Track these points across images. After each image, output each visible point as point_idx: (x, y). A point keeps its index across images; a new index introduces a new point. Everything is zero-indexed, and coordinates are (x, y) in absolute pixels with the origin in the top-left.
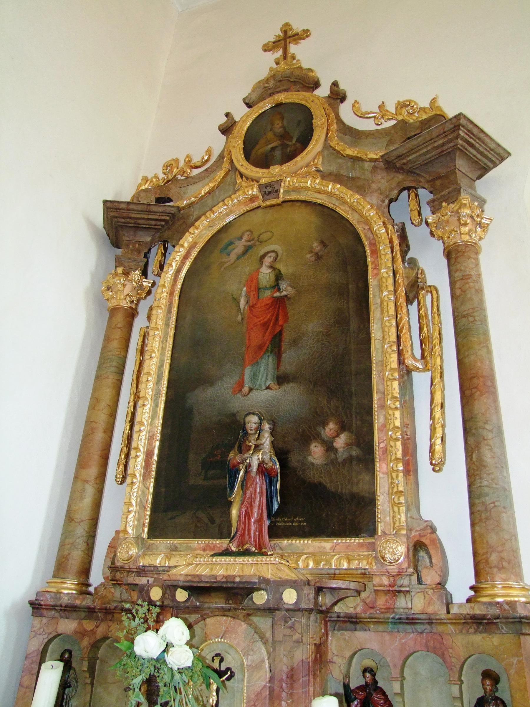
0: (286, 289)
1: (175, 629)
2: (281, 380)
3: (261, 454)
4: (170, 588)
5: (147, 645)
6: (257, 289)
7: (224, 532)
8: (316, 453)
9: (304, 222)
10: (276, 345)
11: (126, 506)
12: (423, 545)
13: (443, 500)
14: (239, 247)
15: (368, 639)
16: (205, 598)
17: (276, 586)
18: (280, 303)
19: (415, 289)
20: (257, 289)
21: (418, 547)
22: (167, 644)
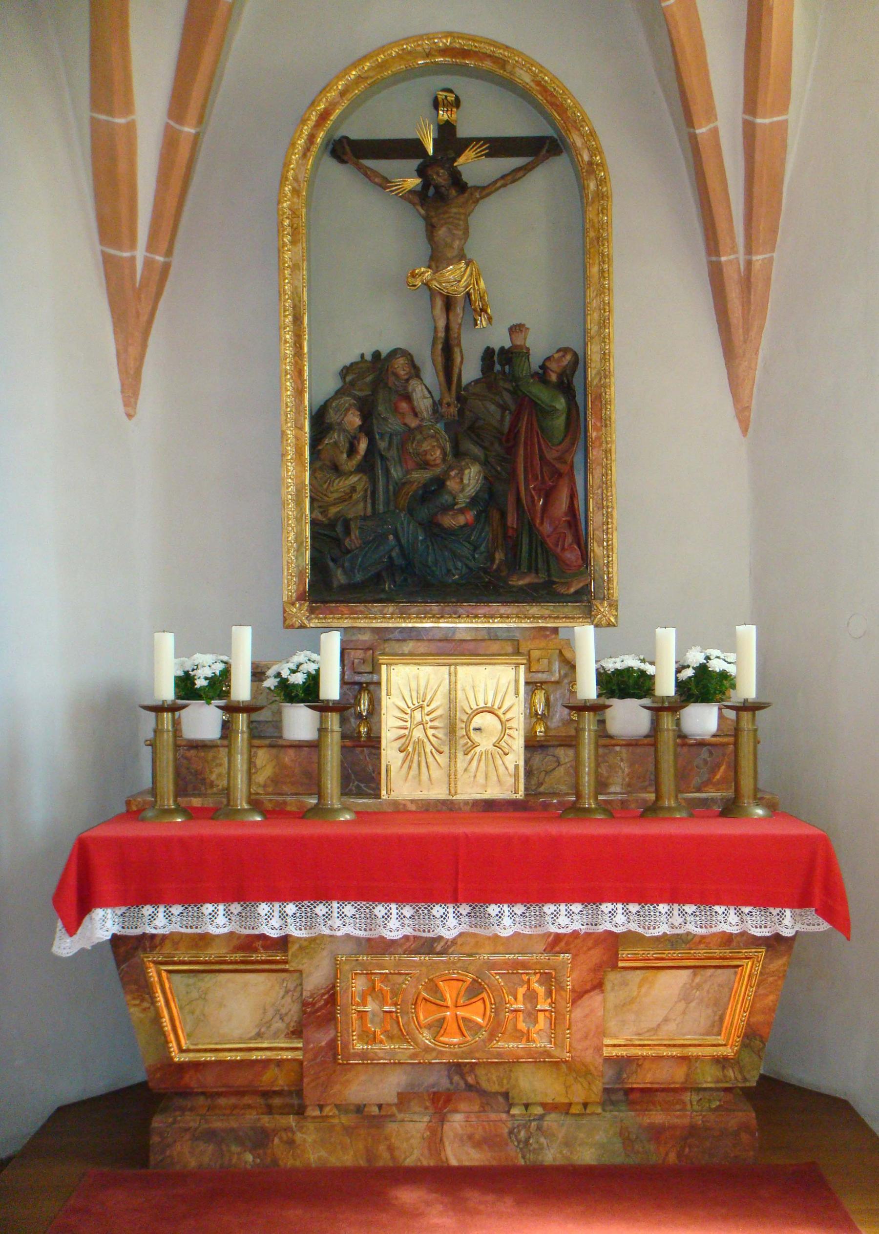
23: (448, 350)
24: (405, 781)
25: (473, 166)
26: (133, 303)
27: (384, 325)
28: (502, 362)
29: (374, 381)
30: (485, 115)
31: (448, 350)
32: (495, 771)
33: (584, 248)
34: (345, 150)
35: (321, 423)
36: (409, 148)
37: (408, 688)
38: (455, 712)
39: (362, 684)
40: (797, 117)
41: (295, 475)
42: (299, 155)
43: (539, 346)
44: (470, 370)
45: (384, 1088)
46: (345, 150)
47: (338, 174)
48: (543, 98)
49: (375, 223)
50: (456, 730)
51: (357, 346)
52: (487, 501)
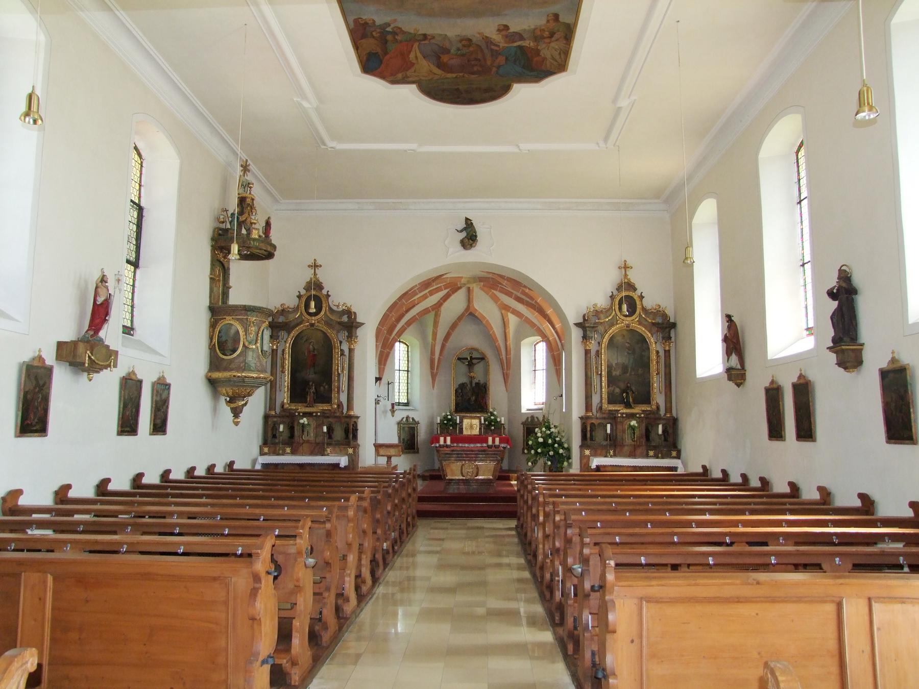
1: (305, 419)
2: (315, 373)
3: (313, 390)
4: (299, 413)
5: (301, 421)
6: (309, 352)
7: (306, 402)
9: (320, 335)
10: (314, 365)
11: (284, 396)
12: (340, 405)
13: (343, 398)
15: (330, 420)
16: (305, 414)
17: (317, 413)
18: (314, 355)
19: (342, 354)
20: (309, 352)
21: (338, 406)
22: (304, 421)
23: (471, 383)
24: (466, 432)
25: (474, 361)
26: (434, 376)
27: (464, 380)
28: (477, 384)
29: (462, 386)
30: (475, 355)
31: (471, 383)
32: (476, 432)
33: (487, 372)
34: (459, 359)
35: (456, 391)
37: (466, 422)
38: (471, 425)
39: (461, 422)
40: (512, 356)
41: (453, 397)
42: (454, 360)
43: (482, 382)
46: (459, 359)
48: (482, 353)
49: (463, 368)
50: (471, 427)
51: (460, 382)
52: (476, 400)
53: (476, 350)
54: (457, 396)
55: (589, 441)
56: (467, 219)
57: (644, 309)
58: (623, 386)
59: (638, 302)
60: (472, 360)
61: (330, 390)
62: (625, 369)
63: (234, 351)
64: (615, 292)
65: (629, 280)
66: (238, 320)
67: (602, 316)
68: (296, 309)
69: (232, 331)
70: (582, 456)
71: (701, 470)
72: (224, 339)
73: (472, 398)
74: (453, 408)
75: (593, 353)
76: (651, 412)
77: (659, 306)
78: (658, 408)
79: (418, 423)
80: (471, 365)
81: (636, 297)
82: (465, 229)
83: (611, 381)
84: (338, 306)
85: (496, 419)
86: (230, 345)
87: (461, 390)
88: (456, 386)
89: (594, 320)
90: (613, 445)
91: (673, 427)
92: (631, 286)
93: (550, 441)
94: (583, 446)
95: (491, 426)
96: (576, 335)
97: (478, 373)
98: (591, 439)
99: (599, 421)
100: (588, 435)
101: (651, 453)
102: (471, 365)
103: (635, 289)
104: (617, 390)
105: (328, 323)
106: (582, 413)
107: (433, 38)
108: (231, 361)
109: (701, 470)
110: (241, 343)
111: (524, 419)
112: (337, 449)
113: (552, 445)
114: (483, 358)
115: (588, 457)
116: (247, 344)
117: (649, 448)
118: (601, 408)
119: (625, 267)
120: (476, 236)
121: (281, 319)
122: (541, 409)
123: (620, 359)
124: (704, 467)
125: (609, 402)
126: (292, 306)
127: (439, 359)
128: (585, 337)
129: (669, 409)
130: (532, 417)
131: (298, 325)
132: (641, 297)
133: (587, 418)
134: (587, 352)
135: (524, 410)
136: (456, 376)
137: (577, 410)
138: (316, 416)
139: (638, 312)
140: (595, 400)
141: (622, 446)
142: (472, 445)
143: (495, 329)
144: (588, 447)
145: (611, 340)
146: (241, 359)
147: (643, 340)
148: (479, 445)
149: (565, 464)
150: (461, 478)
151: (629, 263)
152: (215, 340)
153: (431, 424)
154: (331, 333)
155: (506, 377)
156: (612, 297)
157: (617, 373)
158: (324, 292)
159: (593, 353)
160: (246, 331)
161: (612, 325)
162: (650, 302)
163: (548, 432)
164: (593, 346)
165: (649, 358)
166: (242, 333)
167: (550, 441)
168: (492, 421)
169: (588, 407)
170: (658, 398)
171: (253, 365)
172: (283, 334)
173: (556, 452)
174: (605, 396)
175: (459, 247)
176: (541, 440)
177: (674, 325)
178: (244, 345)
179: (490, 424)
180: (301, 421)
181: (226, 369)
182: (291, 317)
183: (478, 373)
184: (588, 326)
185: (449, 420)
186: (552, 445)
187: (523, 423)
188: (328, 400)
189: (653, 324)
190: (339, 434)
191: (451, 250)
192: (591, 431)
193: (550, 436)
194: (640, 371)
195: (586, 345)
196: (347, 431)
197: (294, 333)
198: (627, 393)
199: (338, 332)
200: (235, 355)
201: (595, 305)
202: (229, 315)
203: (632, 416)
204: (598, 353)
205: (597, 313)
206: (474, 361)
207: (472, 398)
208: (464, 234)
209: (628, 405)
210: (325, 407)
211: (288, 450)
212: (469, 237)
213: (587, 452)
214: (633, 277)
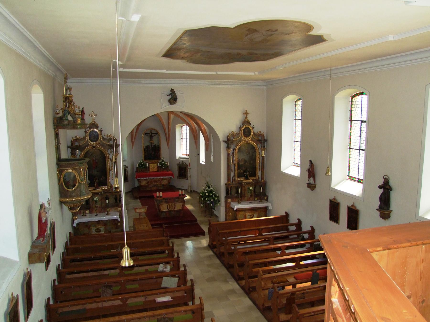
0: (97, 161)
2: (97, 171)
3: (97, 181)
8: (102, 179)
14: (90, 154)
15: (107, 194)
17: (101, 192)
23: (152, 145)
25: (153, 135)
26: (133, 143)
27: (148, 144)
28: (155, 146)
29: (147, 147)
30: (153, 132)
31: (152, 145)
32: (155, 170)
34: (145, 134)
36: (149, 134)
38: (153, 167)
40: (171, 132)
41: (143, 153)
44: (153, 146)
45: (151, 186)
46: (145, 134)
47: (145, 136)
48: (157, 131)
49: (148, 138)
53: (154, 129)
54: (145, 152)
55: (230, 195)
56: (172, 90)
57: (254, 133)
58: (244, 169)
59: (252, 130)
60: (151, 134)
61: (106, 179)
62: (245, 161)
63: (74, 186)
64: (242, 126)
65: (248, 119)
66: (74, 169)
67: (236, 137)
68: (84, 138)
69: (72, 176)
70: (226, 202)
71: (285, 214)
72: (68, 180)
73: (152, 152)
74: (143, 158)
75: (231, 154)
76: (256, 180)
77: (261, 132)
78: (259, 178)
79: (127, 167)
80: (151, 137)
81: (251, 128)
82: (171, 94)
83: (239, 167)
84: (107, 136)
85: (165, 163)
86: (71, 183)
87: (147, 149)
88: (144, 147)
89: (232, 138)
90: (240, 198)
91: (264, 185)
92: (249, 123)
93: (211, 195)
94: (226, 198)
95: (164, 168)
96: (223, 146)
97: (155, 140)
98: (231, 194)
99: (233, 185)
100: (229, 192)
101: (256, 199)
102: (151, 137)
103: (250, 124)
104: (242, 171)
105: (102, 145)
106: (226, 181)
107: (212, 52)
108: (73, 192)
109: (285, 214)
110: (78, 181)
111: (178, 163)
112: (113, 209)
113: (212, 196)
114: (157, 133)
115: (230, 203)
116: (80, 181)
117: (256, 196)
118: (235, 179)
119: (246, 113)
120: (177, 99)
121: (77, 144)
122: (188, 158)
123: (244, 157)
124: (286, 212)
125: (239, 176)
126: (82, 137)
127: (135, 135)
128: (228, 147)
129: (263, 178)
130: (182, 162)
131: (85, 147)
132: (253, 128)
133: (229, 184)
134: (229, 154)
135: (177, 158)
136: (145, 142)
137: (223, 180)
138: (101, 194)
139: (251, 135)
140: (232, 175)
141: (244, 197)
142: (155, 178)
143: (163, 120)
144: (229, 198)
145: (239, 148)
146: (78, 189)
147: (253, 148)
148: (159, 177)
149: (218, 204)
150: (167, 210)
151: (248, 112)
152: (62, 180)
153: (133, 166)
154: (104, 150)
155: (168, 142)
156: (240, 128)
157: (241, 163)
158: (99, 129)
159: (231, 154)
160: (79, 175)
161: (240, 141)
162: (256, 130)
163: (209, 190)
164: (231, 151)
165: (255, 156)
166: (77, 176)
167: (211, 195)
168: (163, 164)
169: (229, 179)
170: (259, 174)
171: (84, 191)
172: (78, 152)
173: (214, 199)
174: (236, 173)
175: (167, 103)
176: (207, 194)
177: (266, 141)
178: (79, 182)
179: (162, 165)
180: (95, 199)
181: (71, 197)
182: (82, 143)
183: (155, 140)
184: (229, 141)
185: (142, 165)
186: (212, 196)
187: (178, 165)
188: (105, 184)
189: (258, 140)
190: (112, 200)
191: (164, 105)
192: (231, 190)
193: (211, 191)
194: (252, 162)
195: (228, 151)
196: (116, 199)
197: (85, 151)
198: (246, 173)
199: (108, 149)
200: (75, 187)
201: (232, 132)
202: (69, 167)
203: (249, 183)
204: (233, 154)
205: (233, 135)
206: (153, 135)
207: (152, 152)
208: (170, 97)
209: (247, 178)
210: (103, 188)
211: (87, 212)
212: (173, 98)
213: (229, 200)
214: (250, 118)
